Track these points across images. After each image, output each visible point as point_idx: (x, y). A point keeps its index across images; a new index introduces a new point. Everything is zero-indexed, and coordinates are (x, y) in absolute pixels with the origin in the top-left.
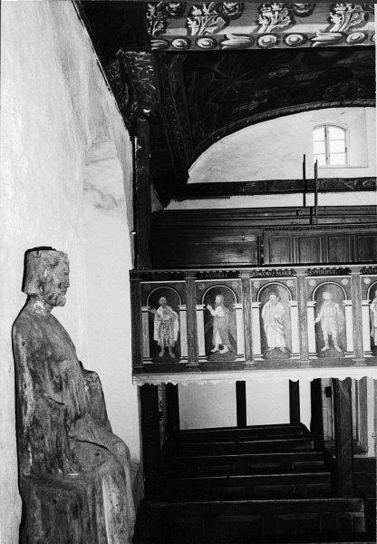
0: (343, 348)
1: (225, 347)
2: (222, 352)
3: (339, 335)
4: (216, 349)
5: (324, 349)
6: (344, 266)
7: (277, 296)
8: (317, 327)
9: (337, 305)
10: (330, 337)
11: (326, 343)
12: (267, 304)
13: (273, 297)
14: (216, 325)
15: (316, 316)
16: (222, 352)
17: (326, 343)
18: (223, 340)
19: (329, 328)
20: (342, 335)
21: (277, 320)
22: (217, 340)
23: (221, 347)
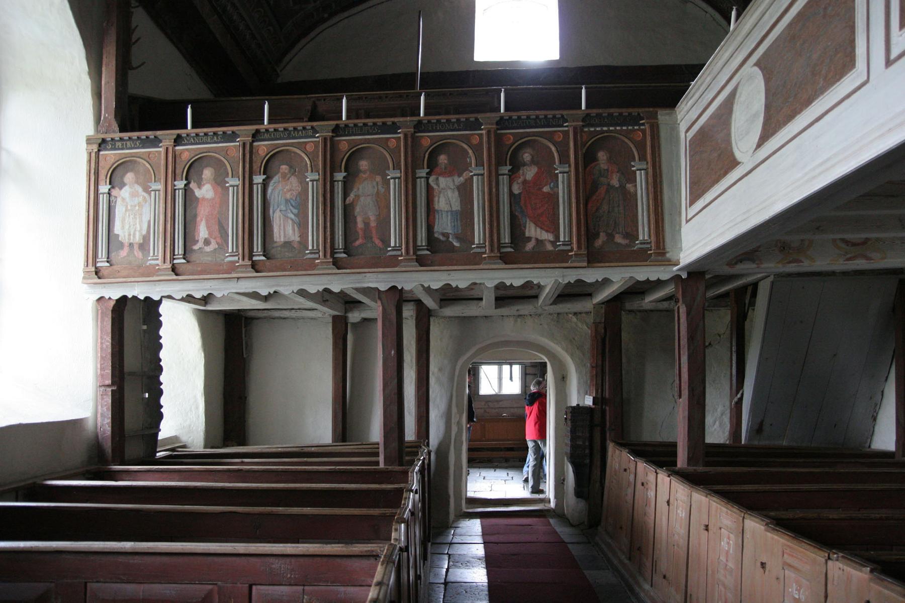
0: (386, 242)
1: (213, 242)
4: (200, 244)
5: (357, 243)
6: (389, 121)
7: (291, 167)
10: (367, 224)
11: (361, 233)
15: (345, 195)
16: (208, 249)
17: (361, 233)
18: (210, 234)
19: (365, 210)
20: (384, 222)
21: (287, 201)
22: (203, 232)
23: (207, 242)
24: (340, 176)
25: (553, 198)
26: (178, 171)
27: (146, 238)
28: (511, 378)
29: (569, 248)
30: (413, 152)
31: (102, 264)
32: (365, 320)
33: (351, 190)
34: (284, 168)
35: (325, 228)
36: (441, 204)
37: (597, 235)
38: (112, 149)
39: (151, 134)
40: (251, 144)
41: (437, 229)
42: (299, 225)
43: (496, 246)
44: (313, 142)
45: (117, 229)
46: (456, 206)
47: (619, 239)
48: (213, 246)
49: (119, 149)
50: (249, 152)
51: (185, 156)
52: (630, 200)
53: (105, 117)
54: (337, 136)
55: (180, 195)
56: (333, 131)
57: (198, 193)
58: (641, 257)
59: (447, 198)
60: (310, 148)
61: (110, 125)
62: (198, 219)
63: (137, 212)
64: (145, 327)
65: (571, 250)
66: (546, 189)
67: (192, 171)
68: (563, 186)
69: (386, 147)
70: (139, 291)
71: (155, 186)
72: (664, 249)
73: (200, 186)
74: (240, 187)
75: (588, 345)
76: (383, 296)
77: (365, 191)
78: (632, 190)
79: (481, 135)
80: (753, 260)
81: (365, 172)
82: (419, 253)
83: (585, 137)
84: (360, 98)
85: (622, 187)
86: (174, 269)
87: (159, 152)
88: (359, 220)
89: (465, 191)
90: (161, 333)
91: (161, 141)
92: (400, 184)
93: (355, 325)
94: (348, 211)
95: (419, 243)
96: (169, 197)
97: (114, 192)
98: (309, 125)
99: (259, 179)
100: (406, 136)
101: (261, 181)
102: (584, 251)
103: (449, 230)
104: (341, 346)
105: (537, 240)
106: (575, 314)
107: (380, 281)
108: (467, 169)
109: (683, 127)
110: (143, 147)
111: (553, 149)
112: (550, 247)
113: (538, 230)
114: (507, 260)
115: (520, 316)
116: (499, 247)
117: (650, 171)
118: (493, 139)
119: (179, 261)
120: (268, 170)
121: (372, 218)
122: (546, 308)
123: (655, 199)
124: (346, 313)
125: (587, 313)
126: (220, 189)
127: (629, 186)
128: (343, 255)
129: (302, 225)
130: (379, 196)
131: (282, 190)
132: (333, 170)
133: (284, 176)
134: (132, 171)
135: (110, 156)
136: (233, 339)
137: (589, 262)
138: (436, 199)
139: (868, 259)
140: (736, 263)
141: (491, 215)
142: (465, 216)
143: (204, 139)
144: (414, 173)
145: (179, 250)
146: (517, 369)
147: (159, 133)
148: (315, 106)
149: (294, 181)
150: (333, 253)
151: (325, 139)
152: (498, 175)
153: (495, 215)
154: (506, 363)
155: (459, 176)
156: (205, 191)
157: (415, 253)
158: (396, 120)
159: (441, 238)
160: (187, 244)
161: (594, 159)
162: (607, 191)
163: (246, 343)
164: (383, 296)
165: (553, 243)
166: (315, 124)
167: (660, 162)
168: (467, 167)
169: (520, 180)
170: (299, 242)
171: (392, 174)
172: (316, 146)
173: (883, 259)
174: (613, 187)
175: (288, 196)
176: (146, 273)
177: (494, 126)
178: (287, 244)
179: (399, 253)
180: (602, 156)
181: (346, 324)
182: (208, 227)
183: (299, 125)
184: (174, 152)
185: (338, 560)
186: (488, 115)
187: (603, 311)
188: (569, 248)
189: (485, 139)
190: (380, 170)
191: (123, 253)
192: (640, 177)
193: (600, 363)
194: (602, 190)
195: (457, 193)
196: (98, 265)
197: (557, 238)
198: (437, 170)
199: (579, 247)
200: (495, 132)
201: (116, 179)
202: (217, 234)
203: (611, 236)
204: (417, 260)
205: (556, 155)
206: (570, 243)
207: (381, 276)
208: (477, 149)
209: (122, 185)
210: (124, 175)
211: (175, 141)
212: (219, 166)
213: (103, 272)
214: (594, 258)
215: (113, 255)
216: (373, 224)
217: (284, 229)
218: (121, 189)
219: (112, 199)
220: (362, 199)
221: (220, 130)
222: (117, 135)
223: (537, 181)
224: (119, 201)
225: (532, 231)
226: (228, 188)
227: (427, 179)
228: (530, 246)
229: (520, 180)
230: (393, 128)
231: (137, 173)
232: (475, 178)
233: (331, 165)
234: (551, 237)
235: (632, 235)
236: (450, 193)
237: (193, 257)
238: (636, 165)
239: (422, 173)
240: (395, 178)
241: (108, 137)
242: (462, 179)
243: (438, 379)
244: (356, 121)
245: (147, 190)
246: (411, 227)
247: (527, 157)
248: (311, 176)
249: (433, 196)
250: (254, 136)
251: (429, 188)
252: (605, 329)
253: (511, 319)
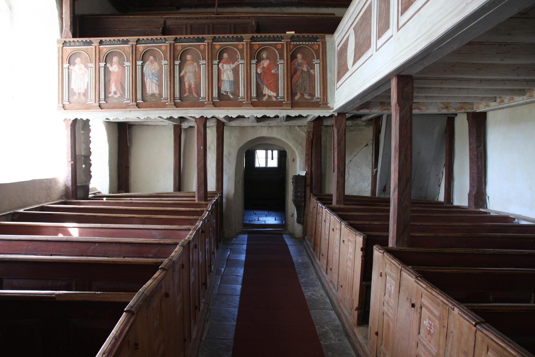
0: (199, 94)
1: (118, 93)
2: (116, 96)
3: (195, 83)
4: (112, 94)
5: (186, 95)
6: (201, 36)
7: (155, 57)
8: (181, 79)
9: (195, 64)
10: (190, 86)
11: (187, 90)
12: (148, 63)
13: (151, 58)
14: (113, 78)
15: (180, 72)
16: (116, 96)
17: (187, 90)
18: (117, 89)
20: (198, 86)
22: (113, 88)
23: (115, 93)
24: (177, 62)
25: (276, 76)
26: (101, 58)
27: (86, 91)
28: (272, 159)
29: (283, 100)
30: (211, 51)
31: (66, 103)
32: (190, 127)
33: (183, 69)
34: (151, 58)
35: (171, 87)
36: (224, 77)
37: (296, 94)
38: (69, 46)
39: (88, 39)
40: (136, 46)
41: (222, 89)
42: (159, 87)
43: (249, 98)
44: (165, 46)
45: (73, 86)
46: (232, 78)
47: (306, 96)
48: (118, 95)
49: (72, 46)
50: (135, 50)
51: (105, 50)
52: (311, 78)
53: (65, 30)
54: (176, 43)
55: (102, 70)
56: (174, 40)
57: (111, 69)
58: (316, 105)
59: (227, 75)
60: (163, 48)
61: (68, 34)
62: (111, 82)
63: (82, 76)
64: (82, 132)
65: (284, 101)
66: (273, 71)
67: (107, 58)
68: (281, 70)
69: (199, 49)
70: (82, 115)
71: (90, 65)
72: (327, 101)
73: (111, 66)
74: (131, 67)
75: (304, 144)
76: (198, 120)
77: (189, 70)
78: (313, 73)
79: (243, 45)
80: (368, 108)
81: (189, 61)
82: (214, 100)
83: (291, 47)
84: (187, 18)
85: (308, 71)
86: (100, 106)
87: (92, 48)
88: (186, 84)
89: (236, 71)
90: (91, 135)
91: (93, 43)
92: (205, 67)
93: (185, 129)
94: (181, 79)
95: (214, 96)
96: (97, 71)
97: (71, 68)
98: (163, 37)
99: (139, 63)
100: (208, 43)
101: (140, 64)
102: (290, 102)
103: (228, 90)
104: (178, 140)
105: (268, 95)
106: (299, 126)
107: (195, 113)
108: (237, 61)
109: (337, 44)
110: (84, 46)
111: (277, 52)
112: (274, 99)
113: (269, 91)
114: (254, 105)
115: (270, 127)
116: (251, 99)
117: (321, 64)
118: (249, 47)
119: (102, 102)
120: (144, 59)
121: (193, 83)
122: (283, 123)
123: (323, 77)
124: (181, 123)
125: (305, 126)
126: (121, 67)
127: (311, 71)
128: (180, 102)
129: (160, 86)
130: (195, 72)
131: (151, 68)
132: (174, 60)
133: (151, 62)
134: (79, 57)
135: (68, 49)
136: (123, 135)
137: (292, 107)
138: (222, 75)
139: (420, 109)
140: (360, 110)
141: (247, 83)
142: (235, 83)
143: (113, 42)
144: (212, 62)
145: (102, 97)
146: (276, 153)
147: (92, 39)
148: (165, 22)
149: (156, 63)
150: (174, 100)
151: (170, 44)
152: (251, 64)
153: (249, 83)
154: (270, 150)
155: (233, 64)
156: (114, 68)
157: (212, 101)
158: (204, 36)
159: (224, 93)
160: (106, 94)
161: (296, 58)
162: (301, 73)
163: (129, 138)
164: (198, 120)
165: (276, 97)
166: (166, 37)
167: (326, 60)
168: (236, 60)
169: (261, 67)
170: (159, 94)
171: (202, 62)
172: (166, 48)
173: (428, 109)
174: (304, 71)
175: (153, 71)
176: (88, 108)
177: (250, 40)
178: (153, 95)
179: (205, 100)
180: (299, 56)
181: (181, 129)
182: (116, 86)
183: (158, 37)
184: (99, 48)
185: (176, 231)
186: (247, 35)
187: (312, 125)
188: (283, 100)
189: (245, 46)
190: (196, 60)
191: (76, 97)
192: (317, 67)
193: (310, 152)
194: (299, 73)
195: (232, 72)
196: (64, 103)
197: (278, 95)
198: (223, 61)
199: (288, 100)
200: (250, 43)
201: (72, 61)
202: (120, 89)
203: (302, 95)
204: (213, 104)
205: (278, 55)
206: (283, 98)
207: (197, 111)
208: (241, 51)
209: (75, 64)
210: (75, 59)
211: (100, 43)
212: (120, 55)
213: (66, 107)
214: (294, 105)
215: (71, 98)
216: (193, 86)
217: (152, 88)
218: (74, 66)
219: (70, 71)
220: (188, 74)
221: (121, 38)
222: (72, 40)
223: (269, 67)
224: (73, 72)
225: (267, 91)
226: (125, 67)
227: (218, 65)
228: (265, 99)
229: (261, 67)
230: (203, 40)
231: (81, 58)
232: (240, 65)
233: (173, 58)
234: (275, 94)
235: (312, 95)
236: (228, 72)
237: (109, 100)
238: (316, 61)
239: (216, 62)
240: (203, 64)
241: (67, 40)
242: (234, 65)
243: (228, 159)
244: (185, 36)
245: (86, 67)
246: (210, 88)
247: (264, 55)
248: (164, 62)
249: (221, 73)
250: (137, 42)
251: (219, 69)
252: (313, 135)
253: (266, 128)
